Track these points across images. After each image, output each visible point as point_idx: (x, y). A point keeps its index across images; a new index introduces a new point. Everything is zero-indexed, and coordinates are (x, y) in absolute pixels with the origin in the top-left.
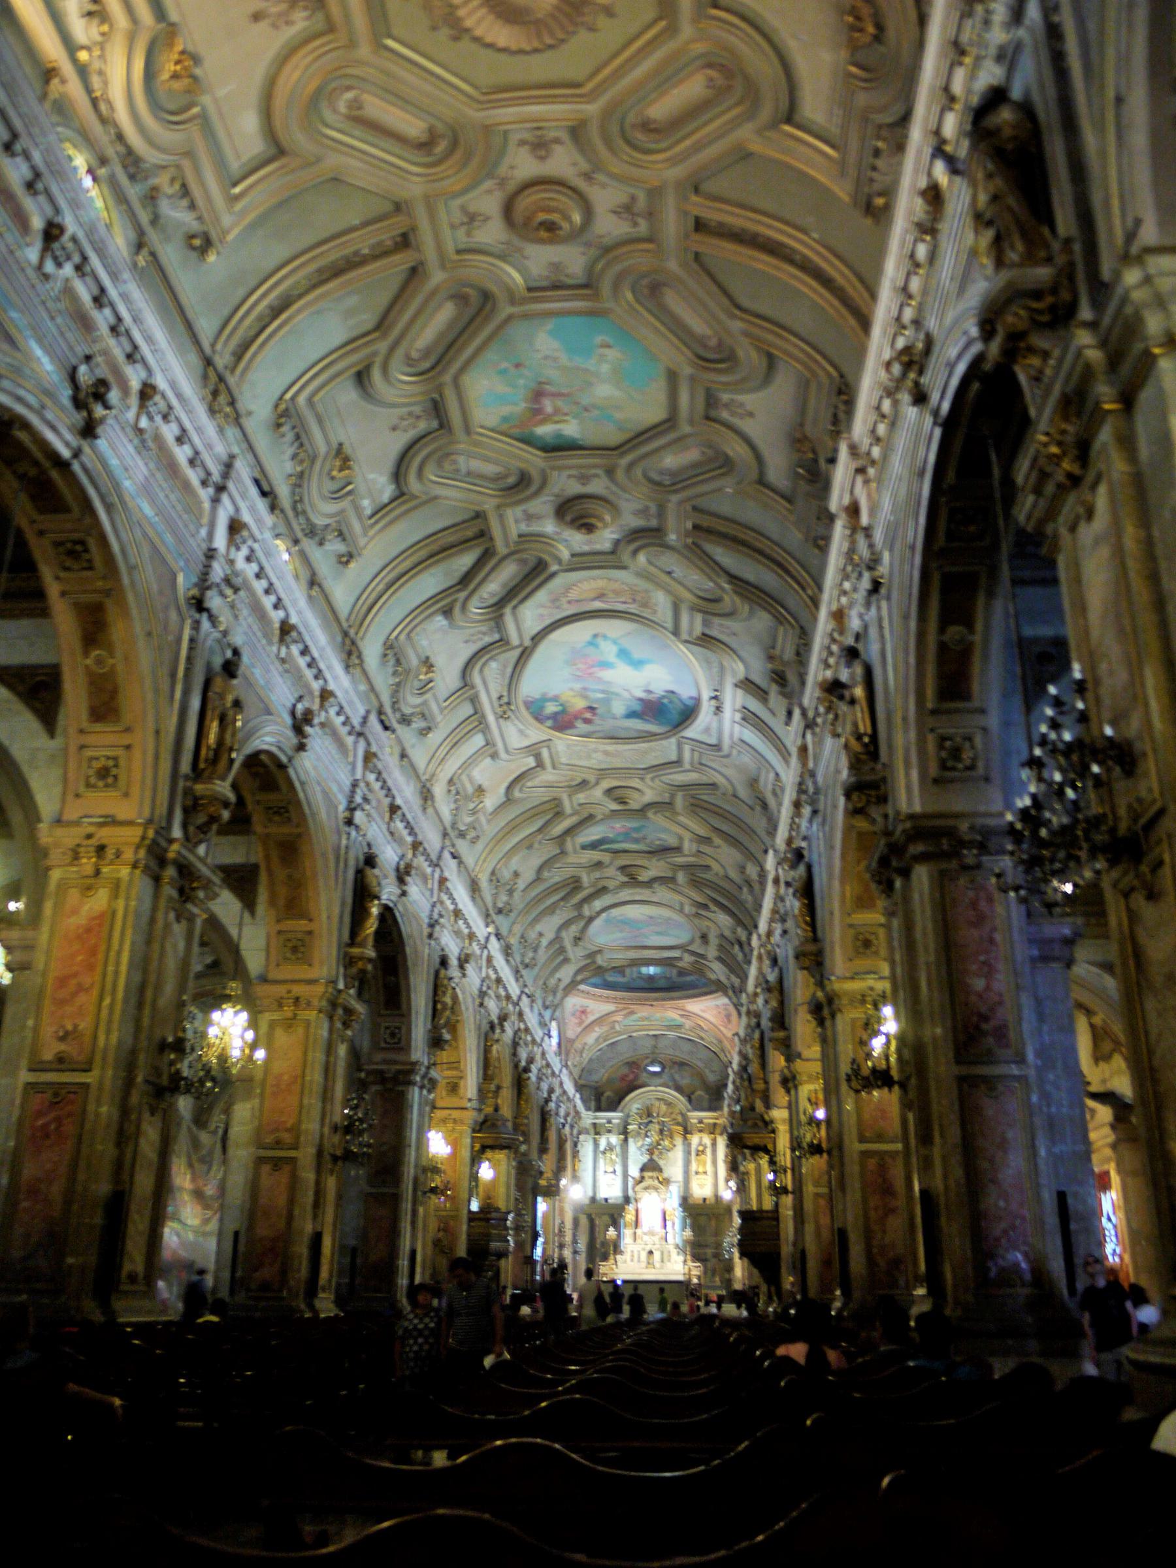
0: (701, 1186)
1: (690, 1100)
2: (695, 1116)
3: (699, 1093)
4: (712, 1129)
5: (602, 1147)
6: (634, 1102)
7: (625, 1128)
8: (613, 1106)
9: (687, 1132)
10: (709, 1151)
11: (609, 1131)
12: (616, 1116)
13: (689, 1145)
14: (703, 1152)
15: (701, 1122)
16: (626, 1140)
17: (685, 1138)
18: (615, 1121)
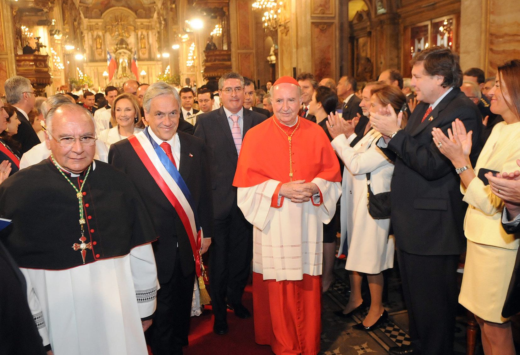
0: (144, 54)
1: (136, 14)
2: (139, 21)
3: (140, 10)
4: (149, 28)
5: (95, 37)
6: (108, 14)
7: (105, 27)
8: (99, 16)
9: (135, 29)
10: (146, 38)
11: (98, 29)
12: (100, 22)
13: (137, 35)
14: (144, 38)
15: (142, 24)
16: (106, 32)
17: (135, 31)
18: (100, 24)
